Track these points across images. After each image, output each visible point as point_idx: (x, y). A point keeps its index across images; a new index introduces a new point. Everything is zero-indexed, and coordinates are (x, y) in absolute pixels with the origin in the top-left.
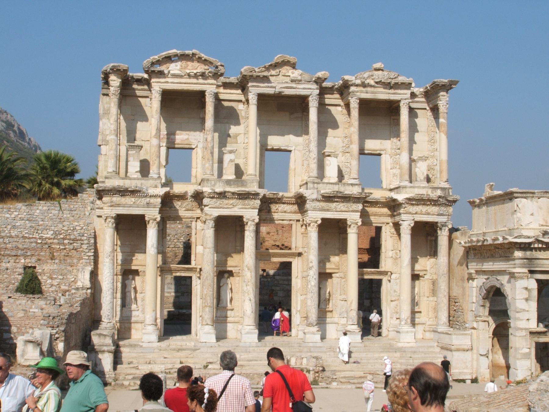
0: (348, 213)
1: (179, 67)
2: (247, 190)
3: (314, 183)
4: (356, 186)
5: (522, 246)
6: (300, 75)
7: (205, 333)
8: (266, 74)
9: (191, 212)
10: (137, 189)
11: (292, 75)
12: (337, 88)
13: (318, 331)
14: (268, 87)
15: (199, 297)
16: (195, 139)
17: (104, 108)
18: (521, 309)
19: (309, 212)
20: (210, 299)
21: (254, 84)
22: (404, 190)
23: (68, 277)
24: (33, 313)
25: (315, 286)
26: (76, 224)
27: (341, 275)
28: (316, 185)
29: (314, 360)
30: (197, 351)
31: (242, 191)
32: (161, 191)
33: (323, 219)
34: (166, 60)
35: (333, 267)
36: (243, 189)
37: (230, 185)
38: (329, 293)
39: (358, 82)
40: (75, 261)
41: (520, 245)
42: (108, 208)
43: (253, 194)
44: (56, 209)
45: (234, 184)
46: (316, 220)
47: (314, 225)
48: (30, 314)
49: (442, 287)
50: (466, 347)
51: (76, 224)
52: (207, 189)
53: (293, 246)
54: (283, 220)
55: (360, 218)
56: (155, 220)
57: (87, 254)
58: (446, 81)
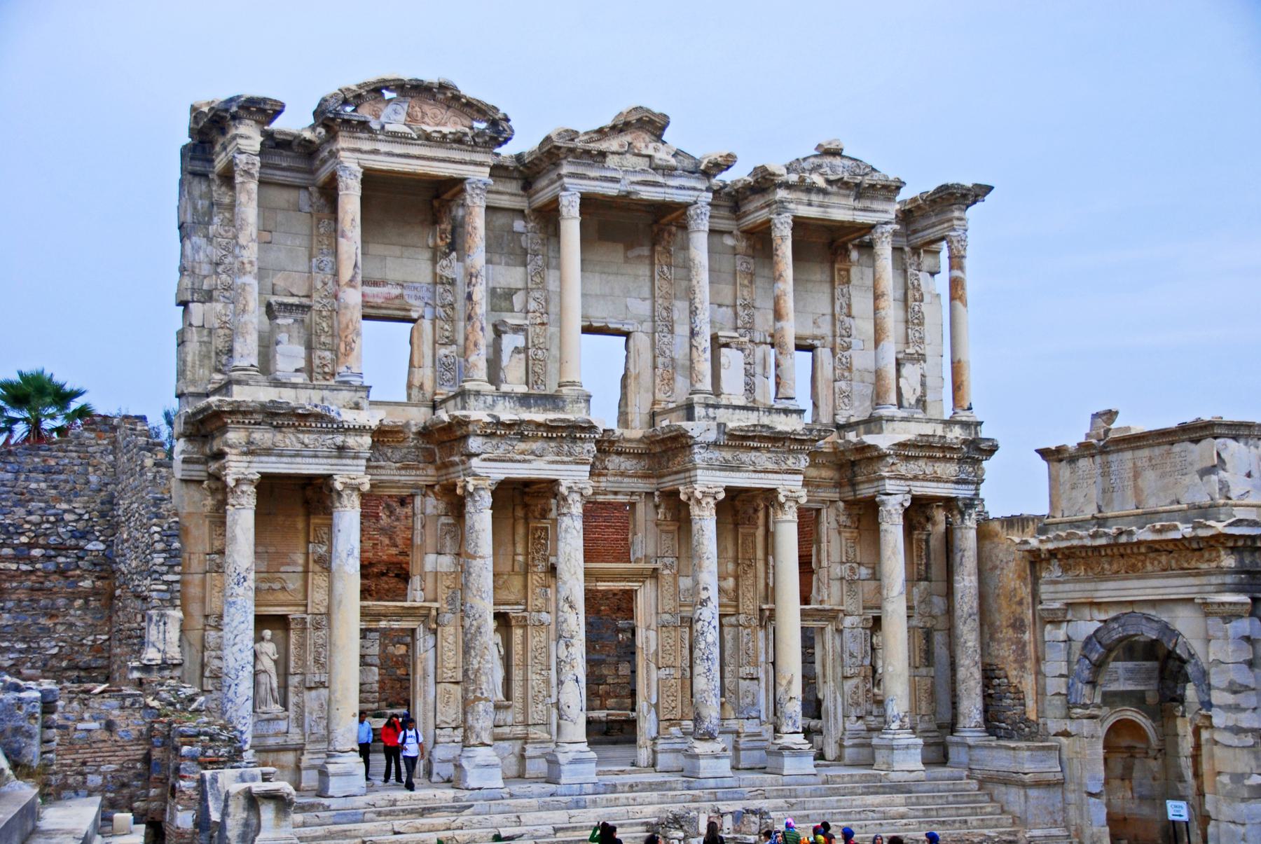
1: (402, 117)
2: (571, 417)
3: (707, 406)
4: (794, 416)
5: (1240, 543)
6: (674, 156)
7: (479, 766)
8: (603, 146)
9: (414, 472)
10: (319, 410)
11: (658, 155)
12: (729, 194)
14: (606, 179)
15: (431, 679)
16: (417, 298)
17: (195, 208)
18: (1241, 685)
19: (699, 472)
21: (572, 169)
22: (891, 425)
23: (42, 644)
24: (84, 734)
25: (714, 643)
26: (65, 506)
28: (711, 410)
29: (755, 819)
30: (467, 812)
33: (728, 490)
34: (373, 95)
35: (725, 600)
36: (562, 416)
37: (529, 407)
39: (793, 178)
40: (61, 602)
41: (1236, 541)
42: (239, 458)
43: (583, 429)
44: (8, 468)
45: (536, 405)
46: (713, 491)
48: (77, 735)
49: (970, 644)
50: (1050, 777)
51: (65, 506)
52: (477, 413)
54: (616, 493)
56: (356, 488)
57: (166, 578)
58: (970, 185)
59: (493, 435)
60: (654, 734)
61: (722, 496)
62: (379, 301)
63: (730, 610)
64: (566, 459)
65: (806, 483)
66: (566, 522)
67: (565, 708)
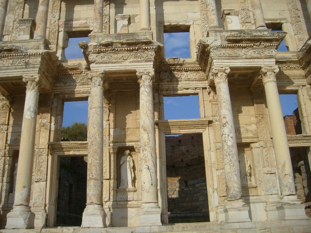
0: (261, 60)
3: (216, 31)
9: (86, 86)
13: (243, 206)
20: (96, 170)
25: (232, 146)
27: (262, 143)
28: (218, 34)
31: (132, 40)
32: (42, 50)
33: (232, 69)
35: (251, 135)
38: (250, 166)
46: (223, 69)
47: (221, 75)
53: (202, 115)
54: (187, 89)
55: (276, 64)
56: (33, 81)
59: (99, 52)
60: (217, 204)
61: (228, 71)
62: (77, 26)
63: (255, 140)
64: (139, 59)
65: (277, 62)
66: (142, 90)
67: (143, 184)
